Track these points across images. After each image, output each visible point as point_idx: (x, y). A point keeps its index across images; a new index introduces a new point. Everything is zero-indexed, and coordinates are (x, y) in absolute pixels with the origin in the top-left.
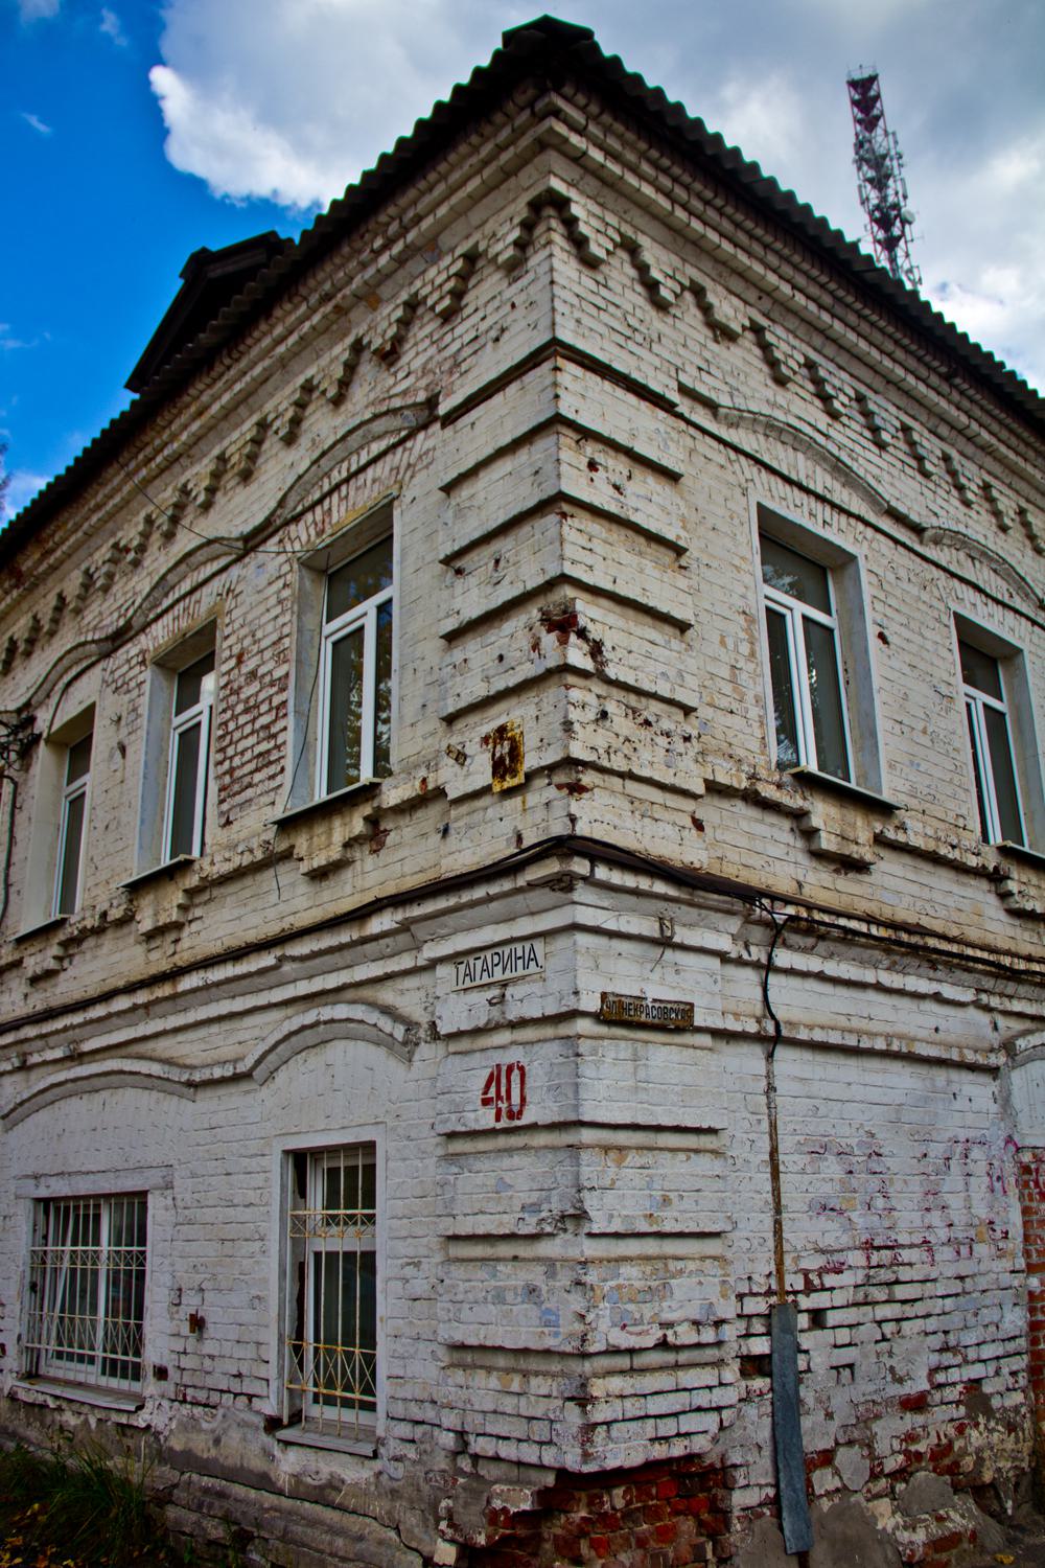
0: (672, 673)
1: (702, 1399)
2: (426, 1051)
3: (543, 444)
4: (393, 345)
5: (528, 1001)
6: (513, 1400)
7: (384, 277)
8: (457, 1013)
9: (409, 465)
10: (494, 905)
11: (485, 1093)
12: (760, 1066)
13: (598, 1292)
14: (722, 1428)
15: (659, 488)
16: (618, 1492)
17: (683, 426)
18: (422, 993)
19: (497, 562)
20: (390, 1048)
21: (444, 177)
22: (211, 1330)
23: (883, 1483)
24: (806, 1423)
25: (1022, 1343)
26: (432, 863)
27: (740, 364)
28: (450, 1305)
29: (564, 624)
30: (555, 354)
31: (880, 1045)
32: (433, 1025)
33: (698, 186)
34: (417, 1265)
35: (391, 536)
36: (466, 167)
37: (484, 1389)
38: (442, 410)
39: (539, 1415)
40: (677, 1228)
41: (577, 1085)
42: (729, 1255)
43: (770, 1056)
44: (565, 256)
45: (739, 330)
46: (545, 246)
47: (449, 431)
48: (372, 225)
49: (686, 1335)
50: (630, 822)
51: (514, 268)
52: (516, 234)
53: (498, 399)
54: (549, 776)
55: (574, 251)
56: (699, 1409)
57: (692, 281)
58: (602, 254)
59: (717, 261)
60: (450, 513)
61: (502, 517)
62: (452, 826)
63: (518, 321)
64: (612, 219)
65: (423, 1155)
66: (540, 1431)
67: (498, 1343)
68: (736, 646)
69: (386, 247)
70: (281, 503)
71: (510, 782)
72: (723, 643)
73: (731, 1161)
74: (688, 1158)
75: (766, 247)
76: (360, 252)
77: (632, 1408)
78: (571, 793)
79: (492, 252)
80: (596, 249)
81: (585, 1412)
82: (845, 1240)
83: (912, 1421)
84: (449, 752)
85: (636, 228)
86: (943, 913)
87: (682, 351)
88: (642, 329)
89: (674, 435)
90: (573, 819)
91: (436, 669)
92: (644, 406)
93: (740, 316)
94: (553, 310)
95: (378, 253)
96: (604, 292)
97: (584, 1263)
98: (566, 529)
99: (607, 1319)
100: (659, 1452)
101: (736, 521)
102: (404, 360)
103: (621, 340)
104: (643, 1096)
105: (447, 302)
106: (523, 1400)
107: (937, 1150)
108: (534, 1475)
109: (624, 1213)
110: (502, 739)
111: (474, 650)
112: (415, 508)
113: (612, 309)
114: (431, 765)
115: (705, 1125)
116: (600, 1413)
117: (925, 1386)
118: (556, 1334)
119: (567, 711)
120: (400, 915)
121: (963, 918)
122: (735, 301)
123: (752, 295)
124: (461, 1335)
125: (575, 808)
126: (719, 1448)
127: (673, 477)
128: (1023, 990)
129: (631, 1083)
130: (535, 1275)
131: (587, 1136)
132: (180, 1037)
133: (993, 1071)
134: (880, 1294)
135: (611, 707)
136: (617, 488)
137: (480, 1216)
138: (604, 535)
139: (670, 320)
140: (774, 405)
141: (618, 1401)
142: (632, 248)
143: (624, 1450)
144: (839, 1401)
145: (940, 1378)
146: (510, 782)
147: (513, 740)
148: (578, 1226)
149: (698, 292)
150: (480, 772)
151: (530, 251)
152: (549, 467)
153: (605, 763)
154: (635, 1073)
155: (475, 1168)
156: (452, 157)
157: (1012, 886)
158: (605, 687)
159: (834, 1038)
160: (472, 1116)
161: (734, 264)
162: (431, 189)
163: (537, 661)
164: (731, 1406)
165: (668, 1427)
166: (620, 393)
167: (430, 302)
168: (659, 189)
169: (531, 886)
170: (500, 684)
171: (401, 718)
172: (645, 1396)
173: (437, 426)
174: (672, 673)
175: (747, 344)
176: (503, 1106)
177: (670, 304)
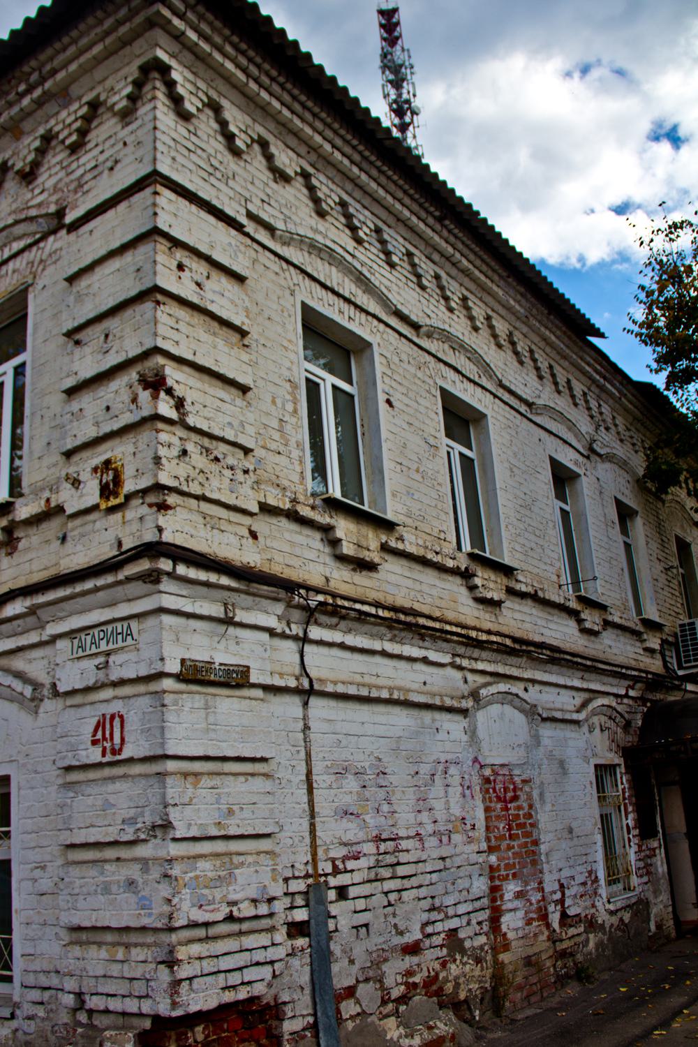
0: (236, 423)
1: (259, 956)
2: (49, 705)
3: (144, 250)
4: (31, 168)
5: (126, 665)
6: (119, 966)
7: (26, 114)
8: (71, 677)
9: (41, 261)
10: (101, 594)
11: (94, 735)
12: (299, 712)
13: (181, 882)
14: (274, 976)
15: (229, 287)
16: (199, 1029)
17: (249, 242)
18: (45, 662)
19: (107, 336)
20: (21, 703)
21: (74, 41)
23: (390, 1006)
24: (335, 968)
25: (485, 901)
26: (53, 562)
27: (292, 199)
28: (69, 898)
29: (156, 384)
30: (156, 182)
31: (385, 694)
32: (54, 685)
33: (266, 66)
34: (43, 868)
35: (25, 316)
36: (92, 35)
37: (96, 959)
38: (68, 219)
39: (138, 976)
40: (239, 832)
41: (163, 728)
42: (277, 850)
43: (306, 704)
44: (165, 110)
45: (293, 174)
46: (150, 100)
47: (73, 236)
48: (17, 74)
49: (247, 910)
50: (203, 532)
51: (126, 115)
52: (129, 89)
54: (143, 498)
55: (172, 106)
56: (258, 964)
57: (259, 136)
58: (193, 110)
59: (278, 122)
60: (72, 298)
61: (111, 303)
62: (69, 535)
63: (128, 156)
64: (201, 84)
66: (139, 988)
67: (106, 924)
68: (283, 405)
69: (29, 91)
71: (113, 502)
72: (274, 402)
73: (278, 781)
74: (247, 780)
75: (315, 115)
76: (8, 93)
78: (159, 510)
79: (110, 102)
80: (190, 105)
81: (172, 972)
82: (361, 835)
83: (410, 961)
84: (67, 478)
85: (220, 94)
86: (429, 600)
87: (250, 186)
88: (221, 168)
89: (242, 248)
90: (160, 530)
91: (58, 415)
92: (221, 225)
93: (293, 165)
94: (155, 149)
95: (21, 96)
96: (193, 138)
97: (170, 861)
98: (159, 313)
99: (188, 902)
101: (286, 314)
102: (40, 180)
103: (205, 175)
104: (212, 735)
105: (74, 137)
106: (126, 966)
107: (425, 769)
108: (135, 1021)
109: (199, 822)
110: (108, 469)
111: (89, 403)
113: (199, 152)
114: (55, 488)
115: (259, 756)
117: (420, 936)
118: (150, 915)
119: (156, 449)
120: (28, 602)
121: (443, 604)
122: (291, 153)
123: (303, 150)
125: (162, 521)
126: (273, 991)
127: (240, 279)
128: (484, 654)
129: (204, 725)
133: (464, 712)
134: (386, 873)
135: (190, 447)
136: (198, 284)
137: (91, 829)
138: (188, 319)
139: (242, 164)
140: (316, 231)
141: (198, 962)
142: (216, 109)
143: (203, 998)
144: (359, 951)
145: (429, 930)
146: (113, 502)
147: (116, 470)
148: (165, 833)
149: (264, 144)
150: (91, 494)
151: (139, 103)
152: (148, 267)
153: (185, 488)
154: (206, 719)
155: (87, 793)
156: (82, 26)
157: (478, 581)
158: (186, 432)
159: (352, 690)
160: (84, 753)
161: (290, 126)
162: (64, 49)
163: (135, 411)
164: (281, 960)
166: (203, 214)
167: (61, 137)
168: (238, 66)
169: (129, 579)
170: (106, 428)
171: (31, 452)
172: (217, 957)
173: (64, 232)
174: (236, 423)
175: (298, 185)
176: (108, 745)
177: (243, 152)
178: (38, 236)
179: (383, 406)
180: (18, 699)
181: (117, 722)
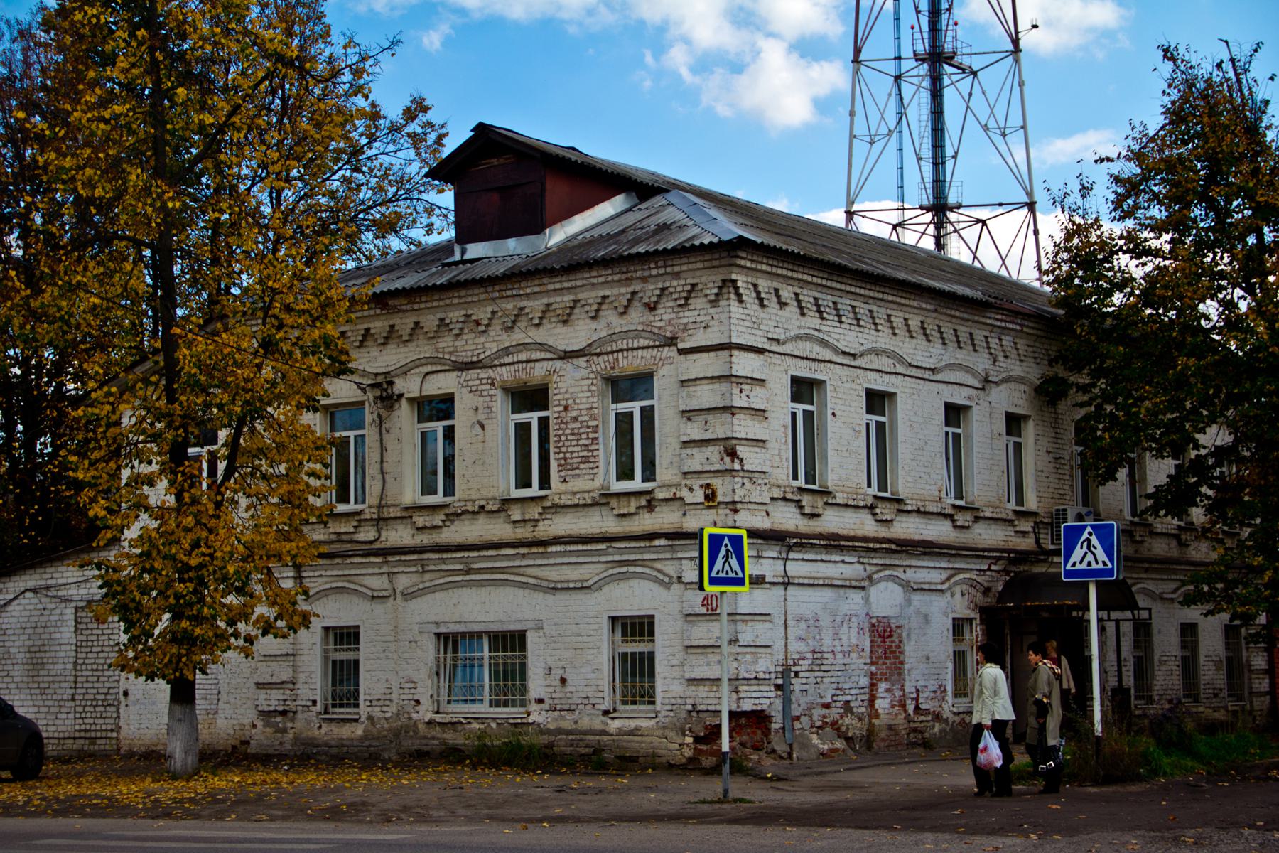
1: (765, 694)
12: (782, 592)
22: (570, 682)
23: (814, 730)
24: (793, 706)
25: (867, 690)
29: (732, 454)
31: (821, 582)
43: (786, 589)
49: (761, 676)
50: (750, 519)
53: (705, 355)
65: (676, 620)
70: (589, 345)
71: (711, 504)
77: (749, 695)
82: (806, 649)
83: (824, 711)
86: (848, 526)
100: (755, 708)
107: (839, 619)
112: (664, 379)
116: (742, 695)
117: (830, 700)
121: (856, 527)
124: (693, 676)
128: (877, 555)
131: (738, 617)
132: (542, 568)
133: (863, 588)
134: (816, 668)
144: (802, 701)
145: (835, 698)
146: (711, 504)
147: (713, 490)
150: (699, 496)
152: (728, 395)
157: (878, 511)
159: (806, 581)
165: (757, 701)
178: (657, 343)
179: (830, 417)
180: (661, 583)
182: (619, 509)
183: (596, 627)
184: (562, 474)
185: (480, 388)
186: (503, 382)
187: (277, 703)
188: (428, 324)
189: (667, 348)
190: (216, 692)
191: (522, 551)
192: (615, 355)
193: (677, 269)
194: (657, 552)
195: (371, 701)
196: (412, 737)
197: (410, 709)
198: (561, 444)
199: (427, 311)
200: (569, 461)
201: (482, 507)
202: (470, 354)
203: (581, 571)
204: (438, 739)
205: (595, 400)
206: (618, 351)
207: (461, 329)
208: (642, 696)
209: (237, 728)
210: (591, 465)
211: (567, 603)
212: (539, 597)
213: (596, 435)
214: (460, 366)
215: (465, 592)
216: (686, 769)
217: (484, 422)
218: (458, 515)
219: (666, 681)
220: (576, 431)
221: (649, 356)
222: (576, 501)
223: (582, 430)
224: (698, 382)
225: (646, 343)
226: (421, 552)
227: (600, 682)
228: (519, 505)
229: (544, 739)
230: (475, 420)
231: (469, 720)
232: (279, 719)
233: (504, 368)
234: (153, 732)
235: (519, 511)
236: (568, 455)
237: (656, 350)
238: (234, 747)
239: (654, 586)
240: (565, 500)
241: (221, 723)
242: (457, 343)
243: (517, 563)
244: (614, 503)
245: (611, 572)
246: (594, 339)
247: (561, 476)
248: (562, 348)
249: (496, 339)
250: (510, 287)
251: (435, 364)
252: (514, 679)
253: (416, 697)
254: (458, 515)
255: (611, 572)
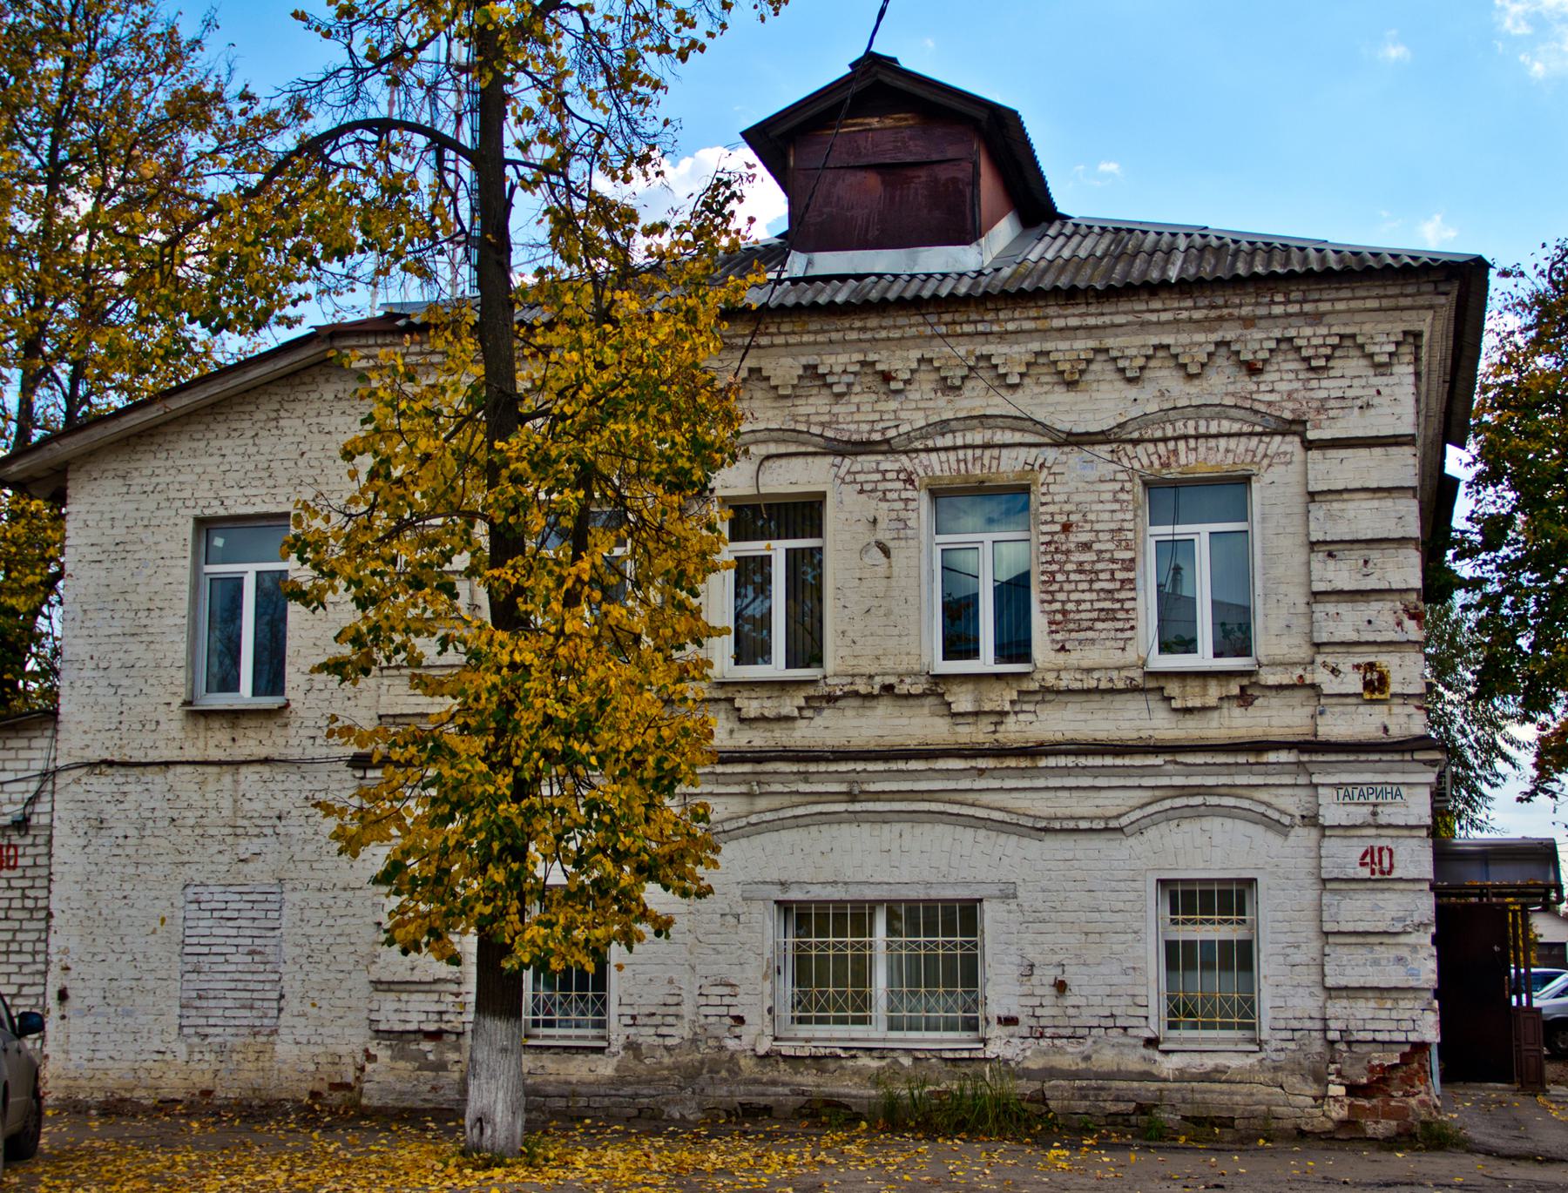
34: (1298, 947)
65: (1300, 888)
112: (1273, 489)
130: (1405, 952)
132: (1015, 795)
146: (1377, 696)
150: (1353, 682)
181: (1385, 854)
182: (1184, 698)
183: (1132, 896)
184: (1058, 637)
185: (881, 486)
186: (934, 478)
187: (423, 1017)
188: (779, 372)
189: (1278, 439)
190: (275, 995)
191: (982, 763)
192: (1171, 445)
193: (1324, 307)
194: (1266, 774)
195: (634, 1017)
196: (725, 1080)
197: (722, 1032)
198: (1055, 587)
199: (783, 351)
200: (1071, 616)
201: (888, 689)
202: (865, 427)
203: (1099, 802)
204: (784, 1084)
205: (1129, 516)
206: (1176, 439)
207: (849, 385)
208: (1190, 1015)
209: (322, 1060)
210: (1120, 625)
211: (1069, 855)
212: (1010, 843)
213: (1131, 575)
214: (841, 447)
215: (847, 832)
216: (1333, 1139)
217: (891, 544)
218: (831, 699)
219: (1280, 991)
220: (1087, 566)
221: (1242, 448)
222: (1093, 684)
223: (1099, 566)
224: (1346, 496)
225: (1236, 427)
226: (759, 761)
227: (1141, 990)
228: (970, 687)
229: (1027, 1087)
230: (873, 540)
231: (852, 1052)
232: (427, 1046)
233: (934, 456)
234: (126, 1065)
235: (970, 697)
236: (1070, 606)
237: (1255, 440)
238: (315, 1095)
239: (1258, 832)
240: (1067, 681)
241: (284, 1049)
242: (835, 409)
243: (965, 784)
244: (1172, 688)
245: (1167, 804)
246: (1133, 415)
247: (1053, 641)
248: (1066, 427)
249: (922, 405)
250: (974, 317)
251: (784, 441)
252: (822, 982)
253: (734, 1012)
254: (831, 699)
255: (1167, 804)
